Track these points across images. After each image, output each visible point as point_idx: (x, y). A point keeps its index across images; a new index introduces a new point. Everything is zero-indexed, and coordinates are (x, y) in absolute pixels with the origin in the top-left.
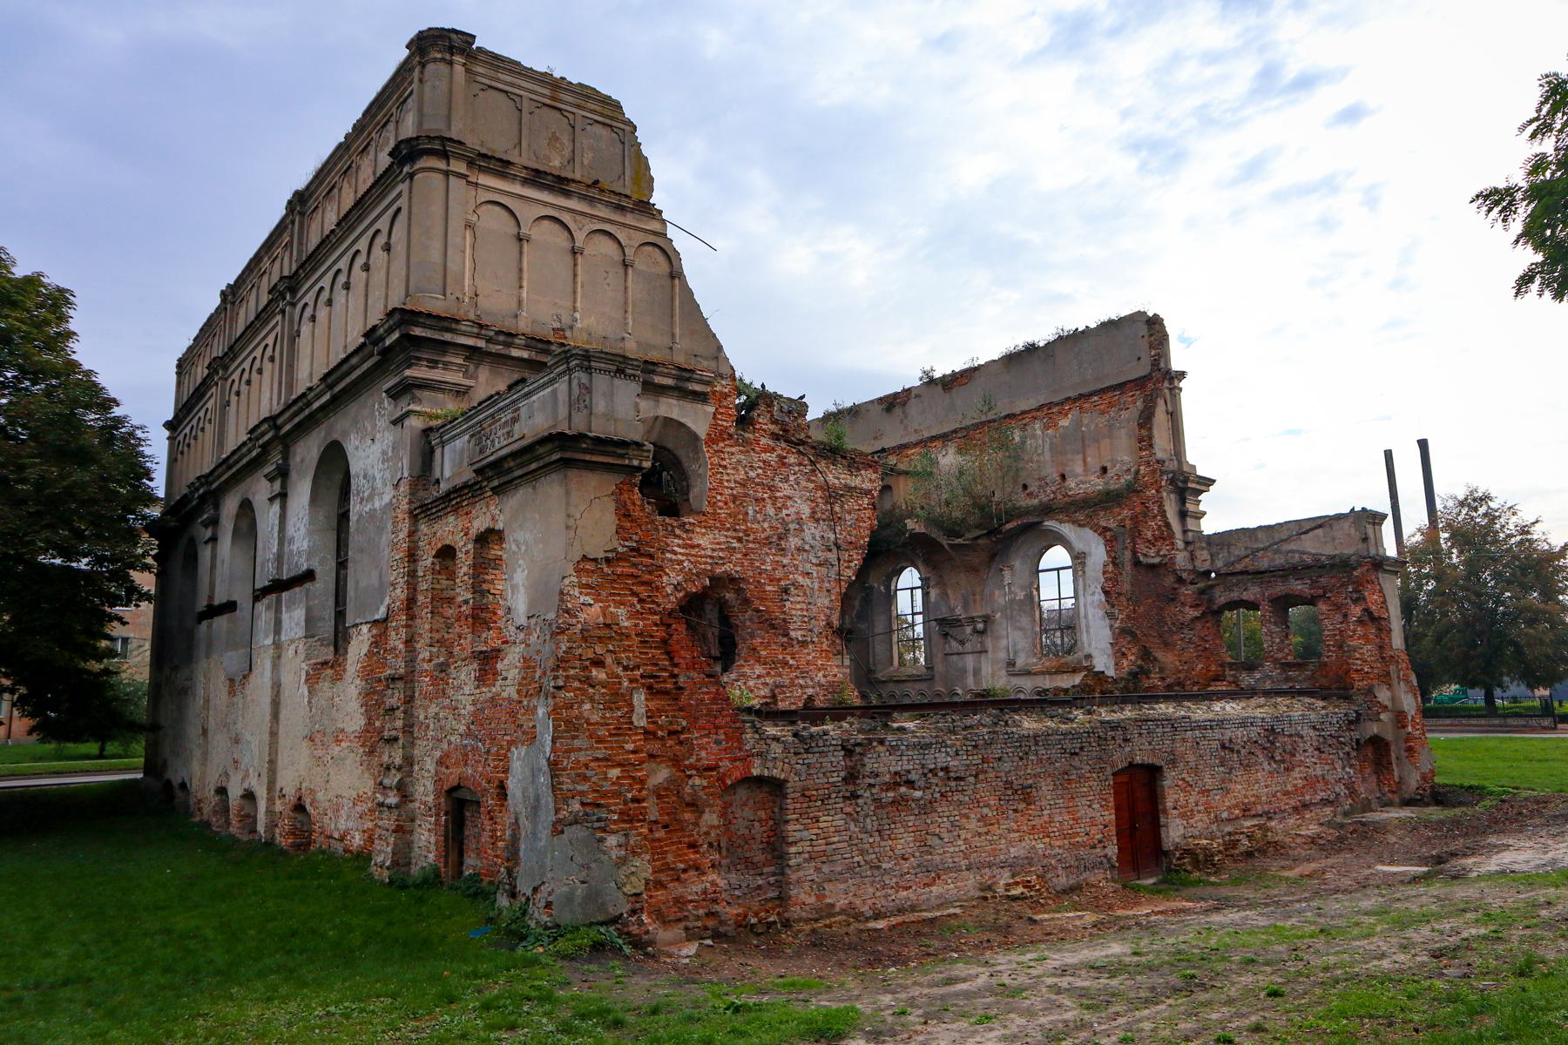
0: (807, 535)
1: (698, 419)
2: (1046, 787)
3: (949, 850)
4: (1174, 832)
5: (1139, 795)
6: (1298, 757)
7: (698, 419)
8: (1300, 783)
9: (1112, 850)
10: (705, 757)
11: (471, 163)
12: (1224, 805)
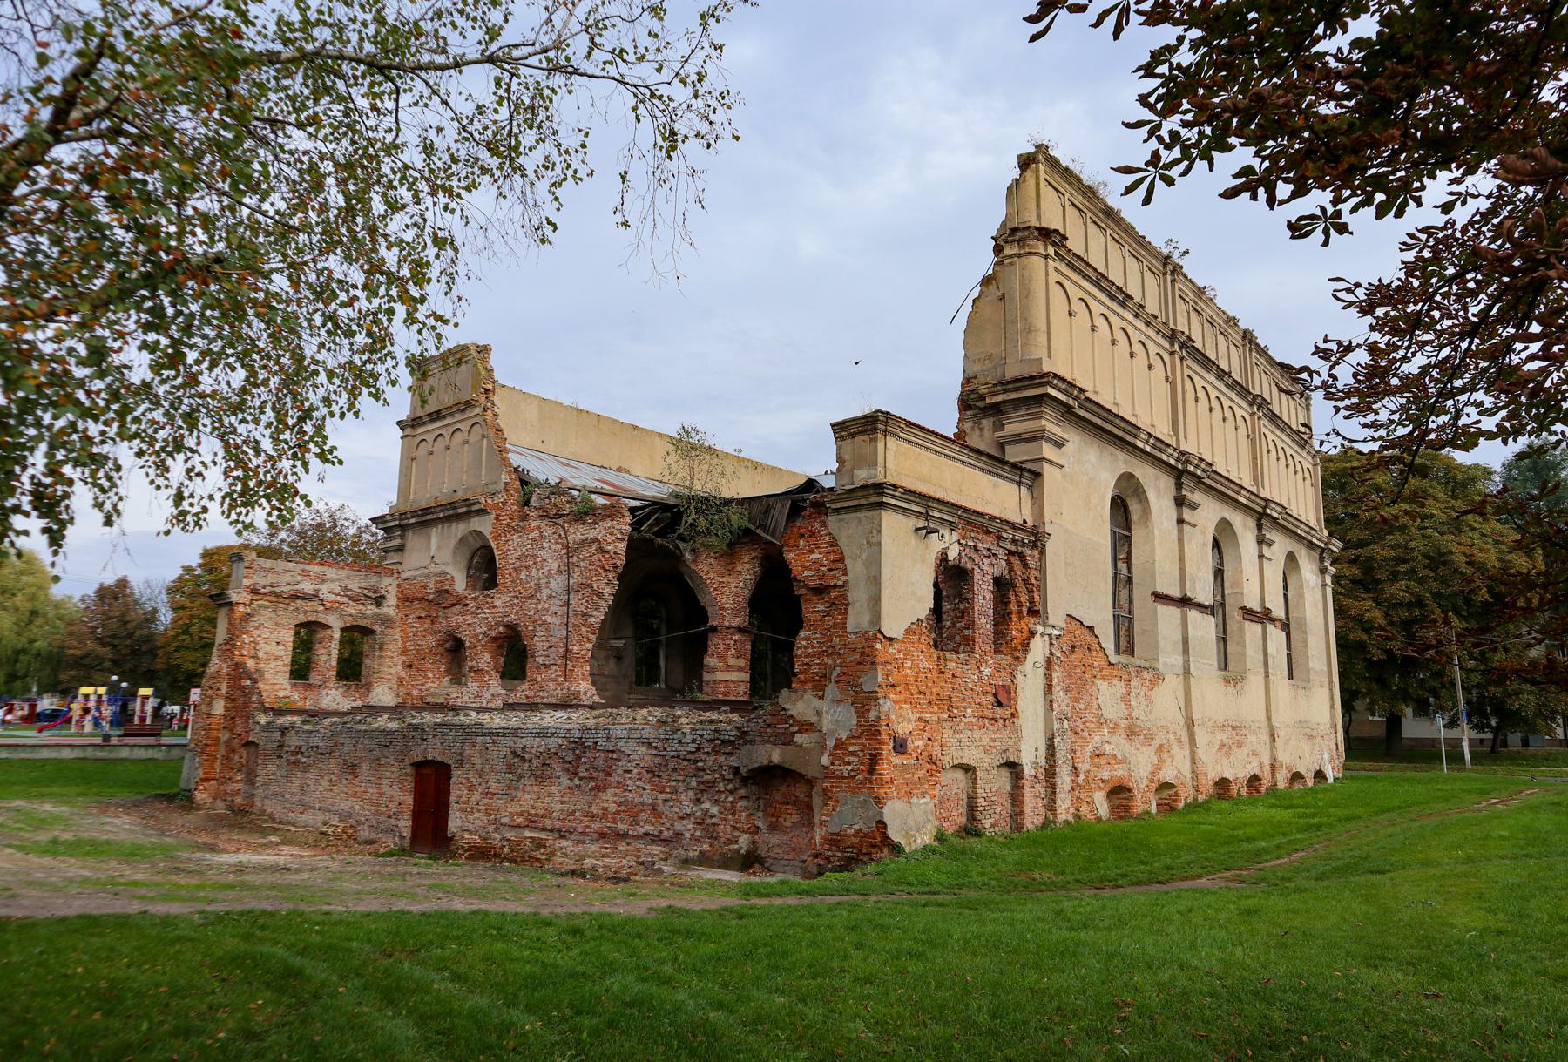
0: (553, 584)
1: (485, 525)
2: (365, 766)
3: (313, 797)
4: (455, 822)
5: (432, 785)
6: (614, 777)
7: (485, 525)
8: (613, 807)
9: (405, 824)
10: (238, 730)
11: (413, 427)
12: (507, 810)
